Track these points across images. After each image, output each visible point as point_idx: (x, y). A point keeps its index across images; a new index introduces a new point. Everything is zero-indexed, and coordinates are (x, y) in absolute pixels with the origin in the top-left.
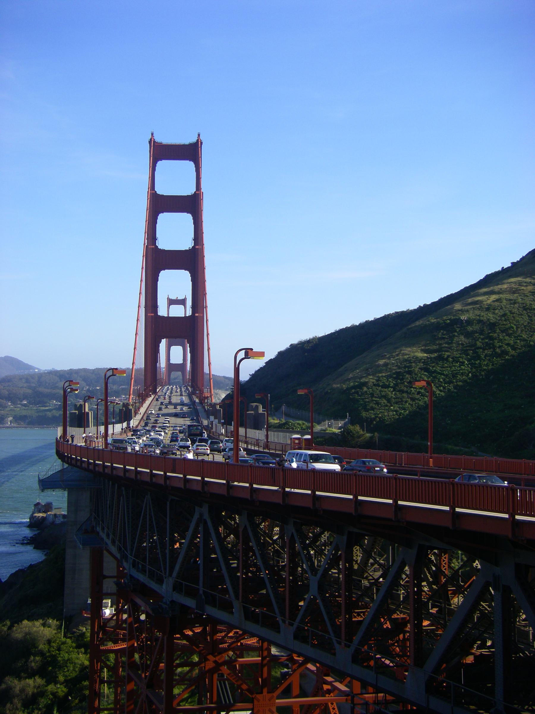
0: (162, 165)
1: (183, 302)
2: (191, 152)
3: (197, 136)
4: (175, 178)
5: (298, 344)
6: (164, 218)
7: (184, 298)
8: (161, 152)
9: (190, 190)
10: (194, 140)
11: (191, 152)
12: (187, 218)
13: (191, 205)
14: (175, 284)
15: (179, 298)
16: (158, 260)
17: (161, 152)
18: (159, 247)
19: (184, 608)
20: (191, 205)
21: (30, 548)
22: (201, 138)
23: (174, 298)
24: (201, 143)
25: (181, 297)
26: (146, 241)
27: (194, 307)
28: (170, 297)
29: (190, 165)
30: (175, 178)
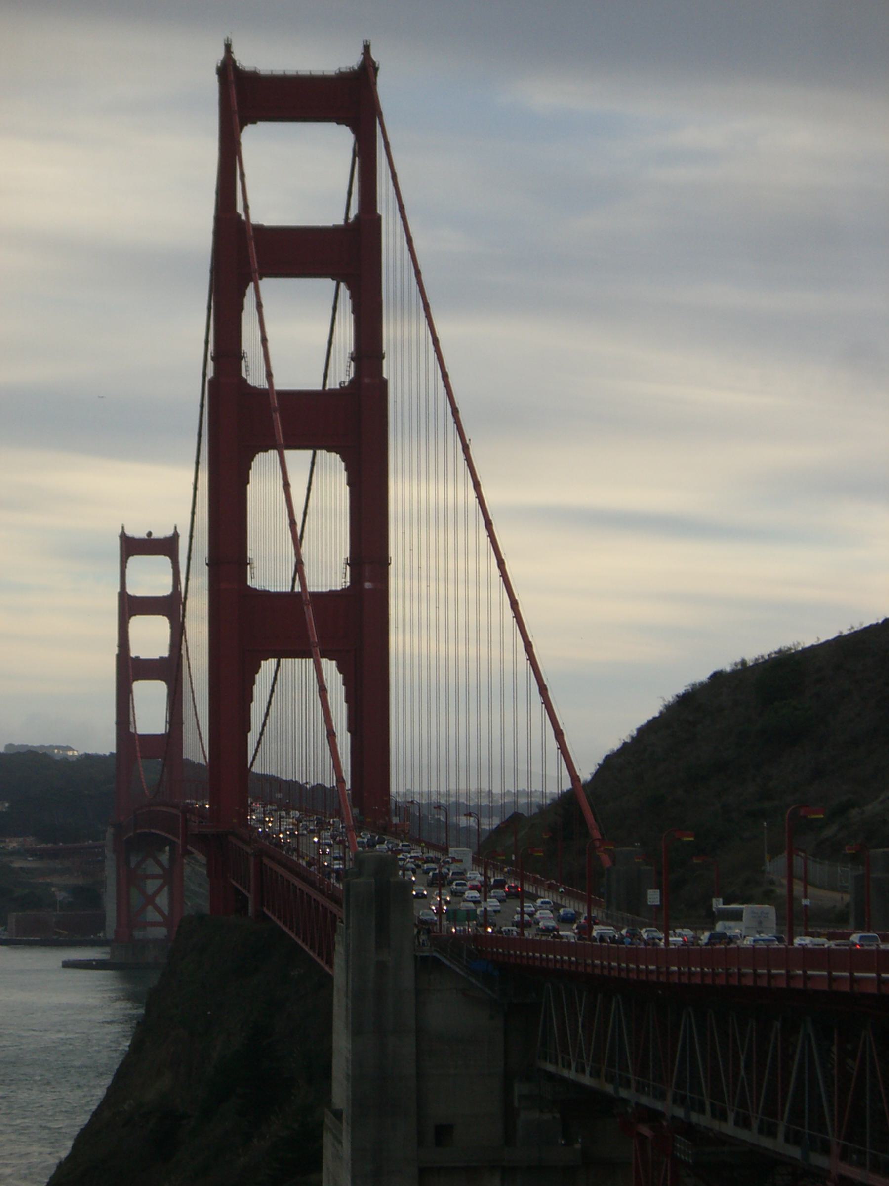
1: (166, 546)
2: (347, 99)
3: (360, 50)
4: (298, 176)
5: (735, 673)
7: (169, 533)
8: (248, 99)
10: (351, 61)
11: (347, 99)
13: (347, 255)
15: (156, 535)
16: (242, 421)
18: (251, 381)
20: (347, 255)
22: (375, 56)
23: (137, 532)
24: (376, 70)
25: (162, 532)
26: (211, 364)
28: (130, 533)
30: (298, 176)
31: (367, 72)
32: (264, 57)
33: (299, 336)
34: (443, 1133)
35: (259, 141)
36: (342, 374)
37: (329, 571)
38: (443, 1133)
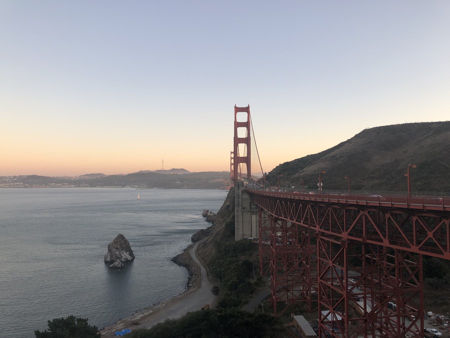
0: (238, 113)
4: (242, 117)
6: (239, 129)
8: (238, 110)
9: (246, 121)
10: (247, 106)
11: (247, 110)
12: (245, 129)
14: (242, 148)
16: (237, 141)
17: (238, 110)
19: (351, 240)
20: (247, 125)
21: (206, 223)
27: (248, 154)
29: (246, 114)
30: (242, 117)
31: (249, 107)
32: (239, 106)
33: (242, 133)
34: (244, 208)
35: (239, 114)
36: (247, 136)
37: (246, 155)
38: (244, 208)
